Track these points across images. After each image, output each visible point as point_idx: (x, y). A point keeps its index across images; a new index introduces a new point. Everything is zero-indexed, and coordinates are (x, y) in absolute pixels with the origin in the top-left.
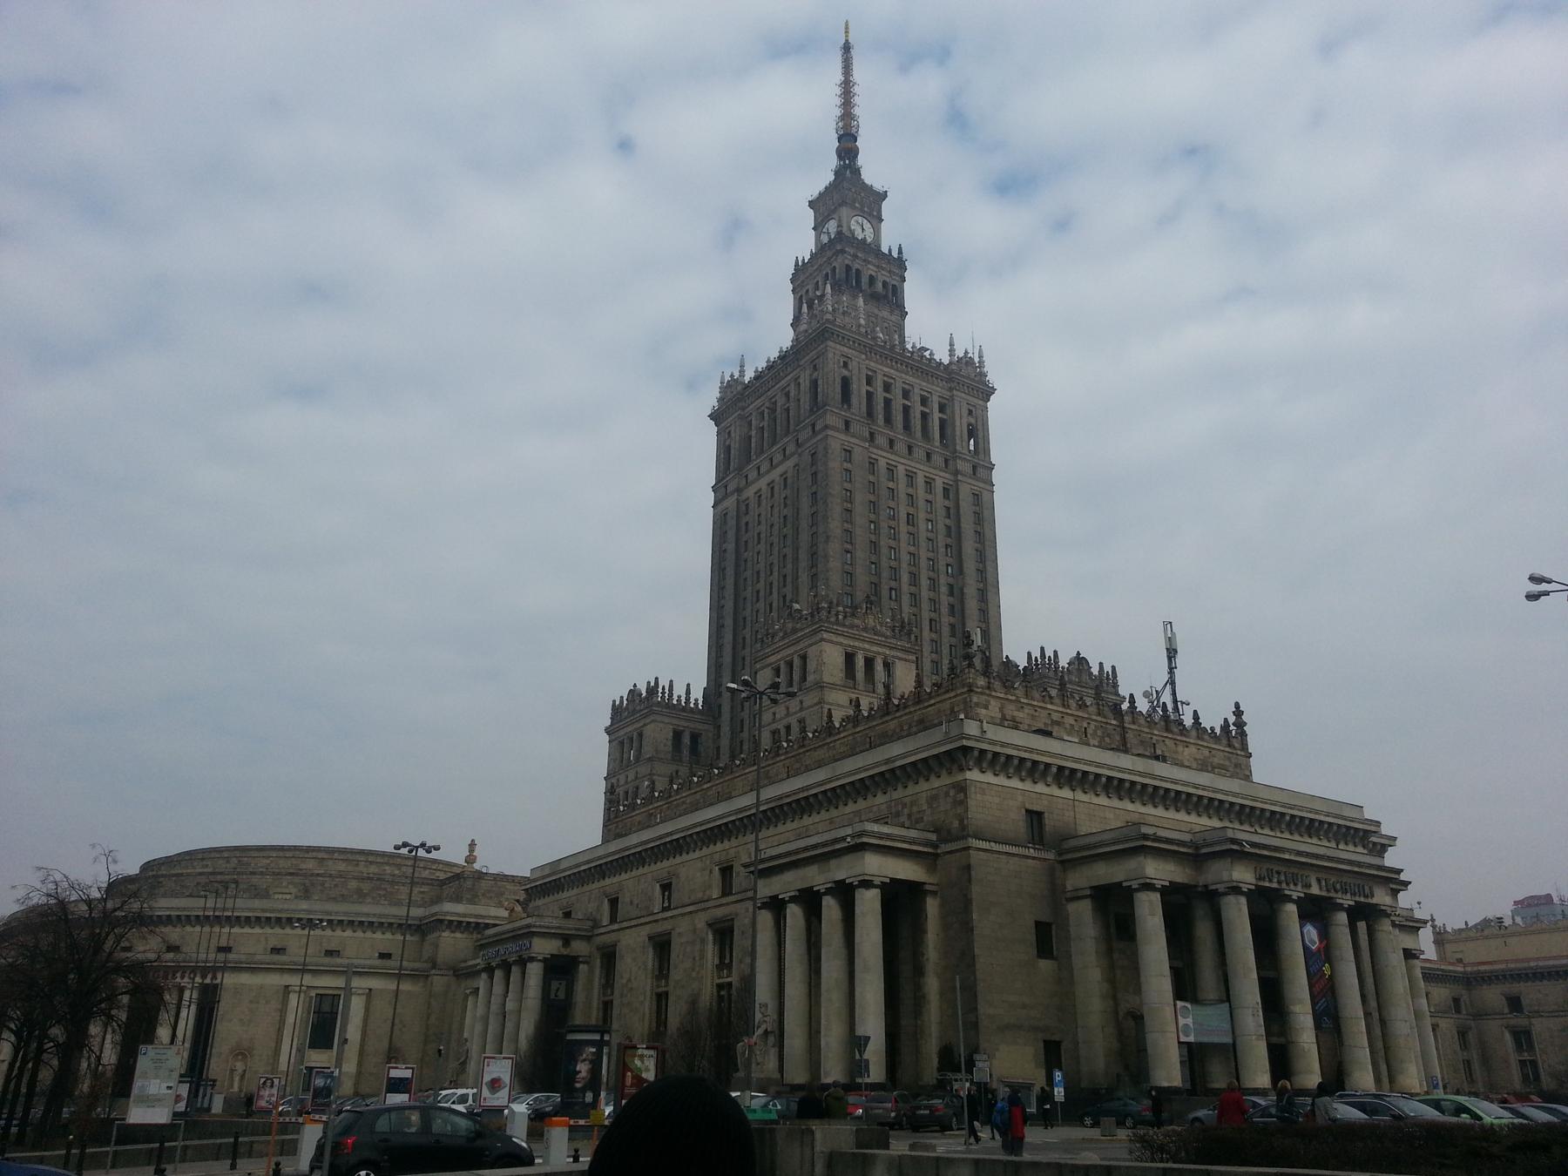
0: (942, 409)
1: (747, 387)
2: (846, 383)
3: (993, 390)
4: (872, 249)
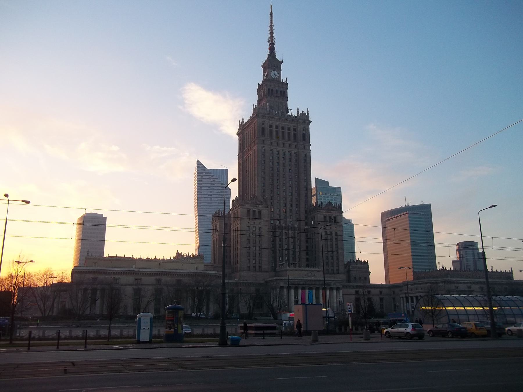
0: (295, 130)
2: (263, 130)
3: (311, 122)
4: (278, 81)
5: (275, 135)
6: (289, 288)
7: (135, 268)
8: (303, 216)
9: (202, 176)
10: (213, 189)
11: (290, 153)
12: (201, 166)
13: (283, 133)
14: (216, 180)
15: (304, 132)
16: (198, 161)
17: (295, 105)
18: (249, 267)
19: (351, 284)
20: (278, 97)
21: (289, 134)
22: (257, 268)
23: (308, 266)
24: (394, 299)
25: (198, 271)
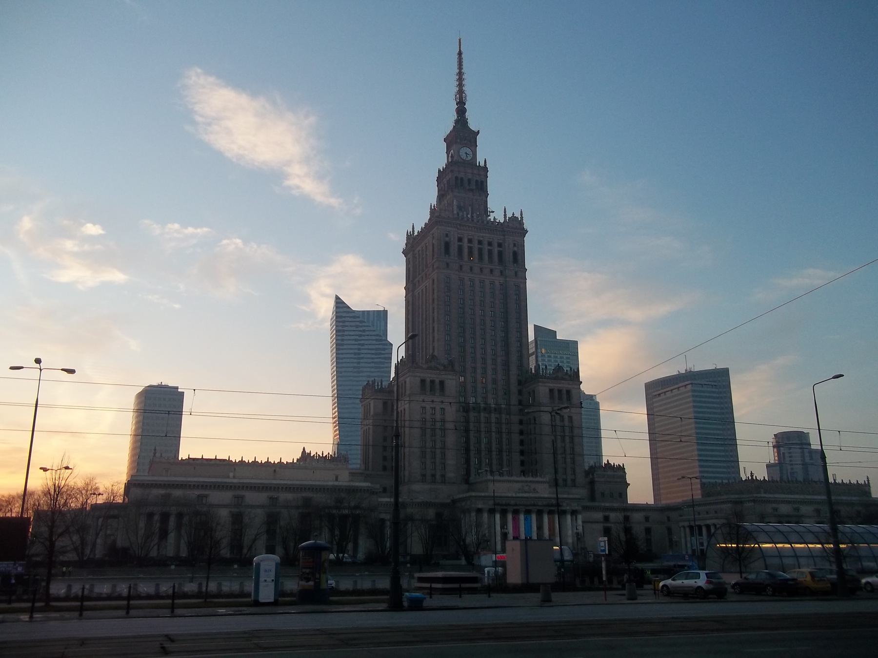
0: (500, 245)
1: (415, 238)
4: (472, 163)
5: (467, 255)
6: (492, 511)
7: (234, 477)
8: (514, 388)
9: (344, 322)
10: (363, 345)
11: (492, 283)
12: (341, 305)
13: (480, 250)
14: (366, 329)
15: (516, 249)
16: (337, 298)
17: (500, 204)
18: (424, 476)
19: (596, 504)
20: (472, 190)
21: (490, 252)
22: (438, 477)
23: (523, 473)
24: (669, 530)
25: (340, 483)
